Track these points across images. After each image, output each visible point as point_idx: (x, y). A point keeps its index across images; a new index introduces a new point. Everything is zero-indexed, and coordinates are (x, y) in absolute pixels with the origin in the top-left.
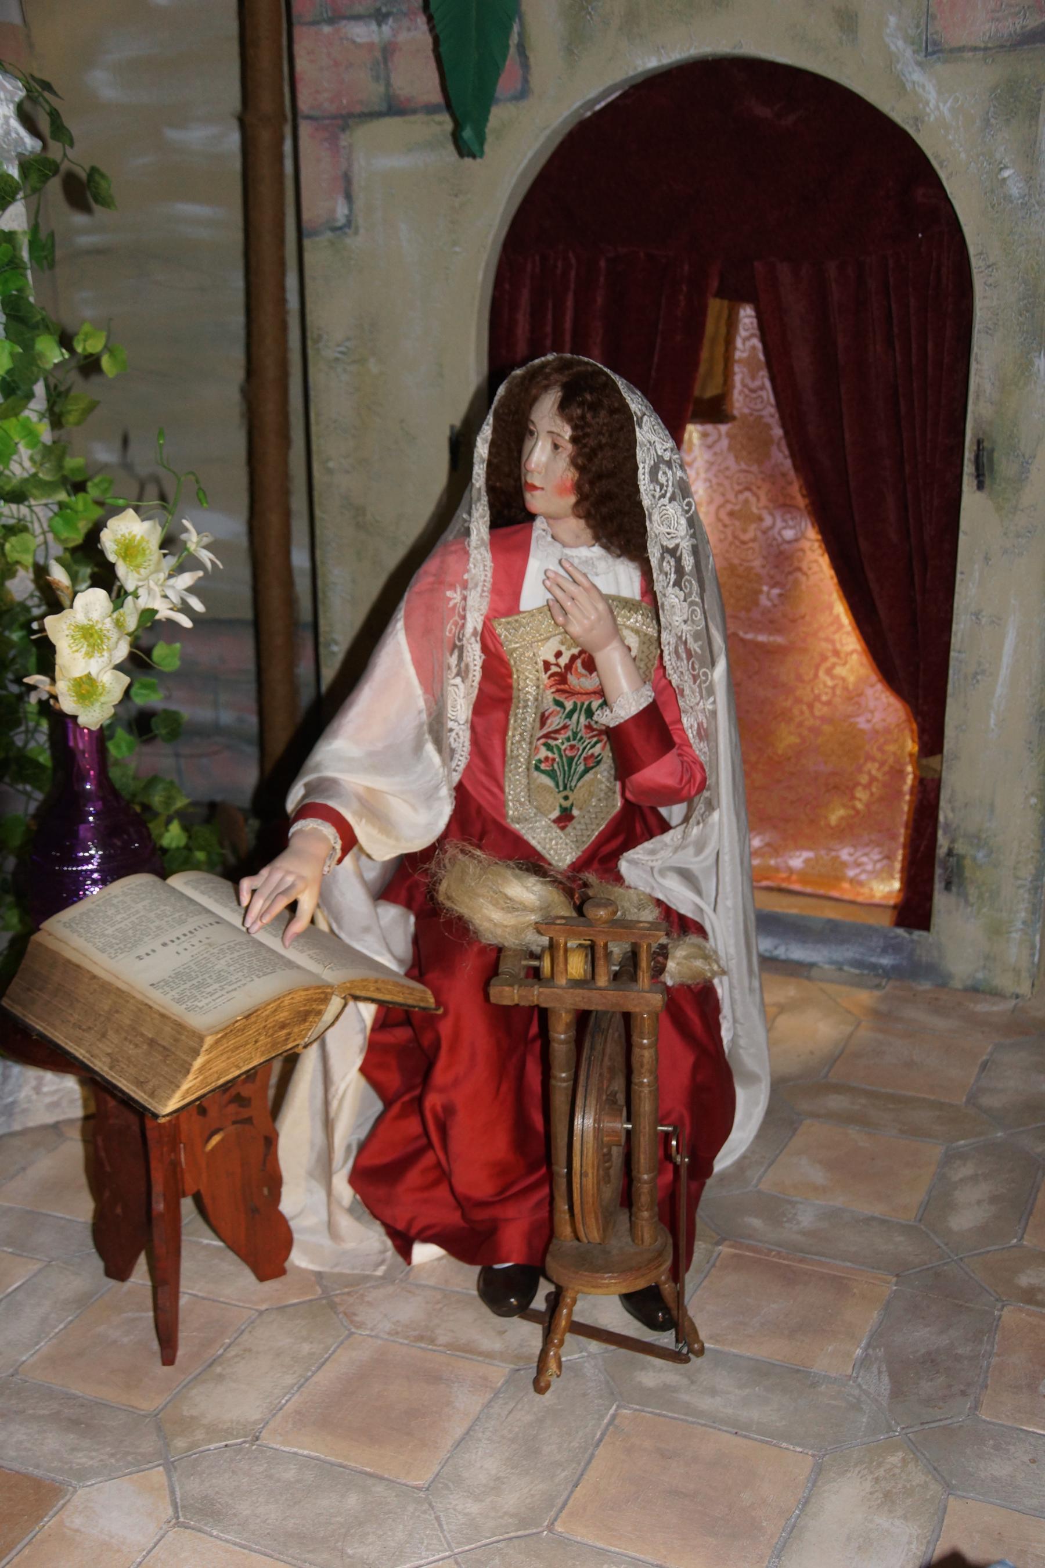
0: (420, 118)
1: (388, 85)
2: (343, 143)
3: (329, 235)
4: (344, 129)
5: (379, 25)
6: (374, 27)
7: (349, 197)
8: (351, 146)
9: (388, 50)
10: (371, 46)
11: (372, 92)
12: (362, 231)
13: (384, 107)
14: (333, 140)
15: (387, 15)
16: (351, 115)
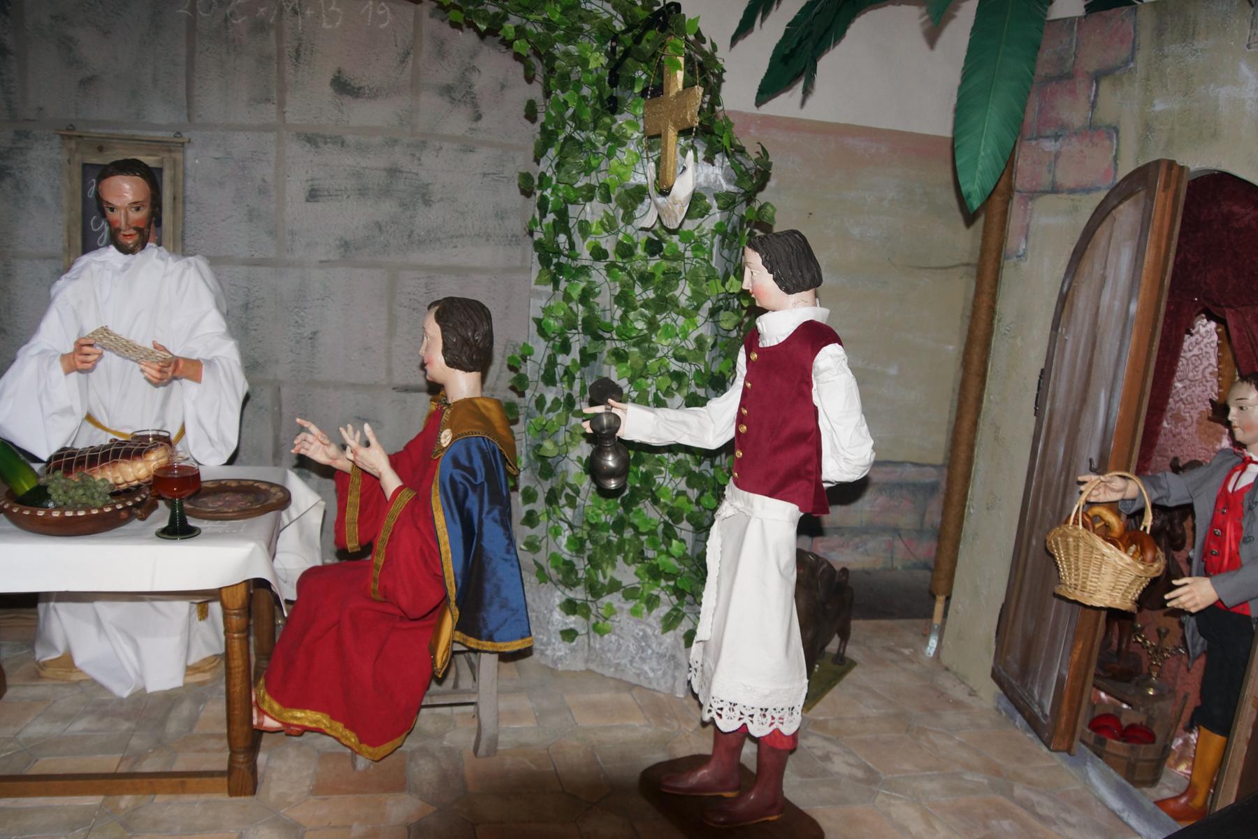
0: (1065, 195)
1: (1054, 176)
2: (1029, 207)
3: (1015, 259)
4: (1031, 199)
5: (1056, 141)
6: (1053, 143)
7: (1026, 238)
8: (1033, 209)
9: (1057, 155)
10: (1050, 153)
11: (1046, 180)
12: (1029, 260)
13: (1050, 189)
14: (1026, 205)
15: (1061, 136)
16: (1035, 192)
